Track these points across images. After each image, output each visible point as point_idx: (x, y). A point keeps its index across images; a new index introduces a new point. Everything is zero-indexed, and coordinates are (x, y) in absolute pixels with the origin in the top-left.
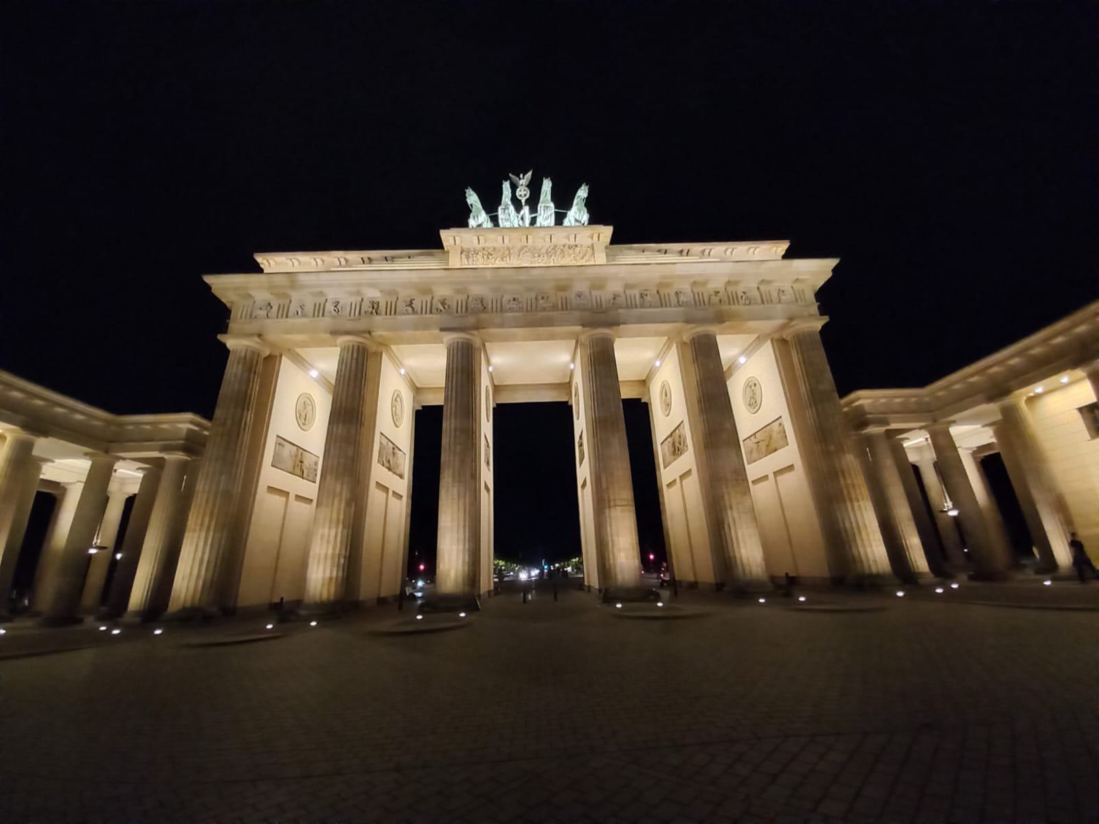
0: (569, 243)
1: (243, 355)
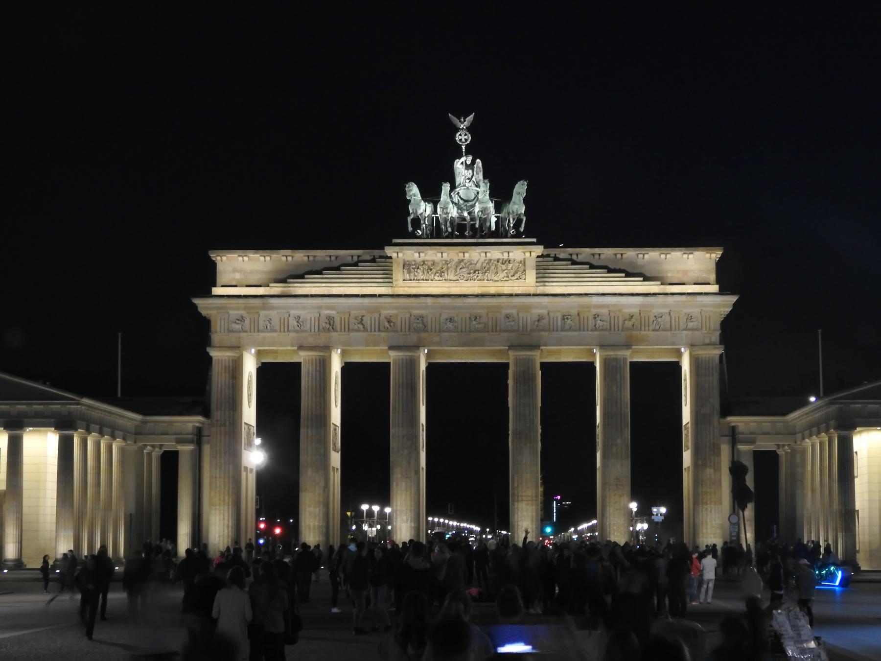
1: (227, 364)
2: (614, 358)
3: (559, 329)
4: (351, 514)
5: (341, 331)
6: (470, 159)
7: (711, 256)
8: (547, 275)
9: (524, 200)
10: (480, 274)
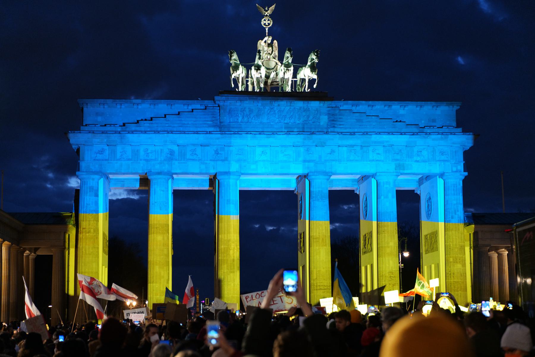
6: (271, 38)
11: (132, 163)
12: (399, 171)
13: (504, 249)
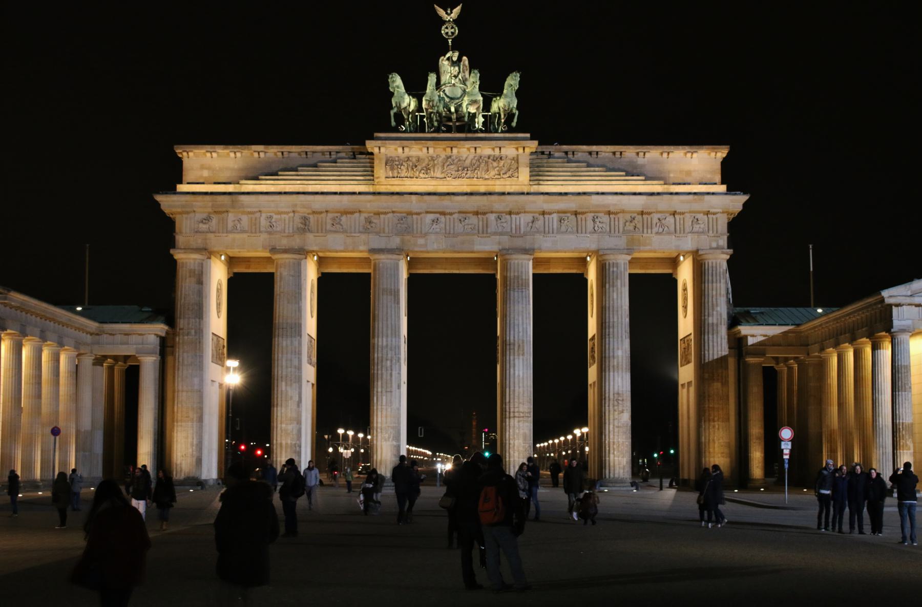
0: (494, 154)
2: (613, 263)
3: (555, 231)
4: (328, 437)
5: (318, 232)
6: (457, 54)
7: (716, 155)
8: (541, 173)
9: (516, 93)
10: (469, 172)
11: (249, 236)
12: (632, 248)
13: (792, 361)
